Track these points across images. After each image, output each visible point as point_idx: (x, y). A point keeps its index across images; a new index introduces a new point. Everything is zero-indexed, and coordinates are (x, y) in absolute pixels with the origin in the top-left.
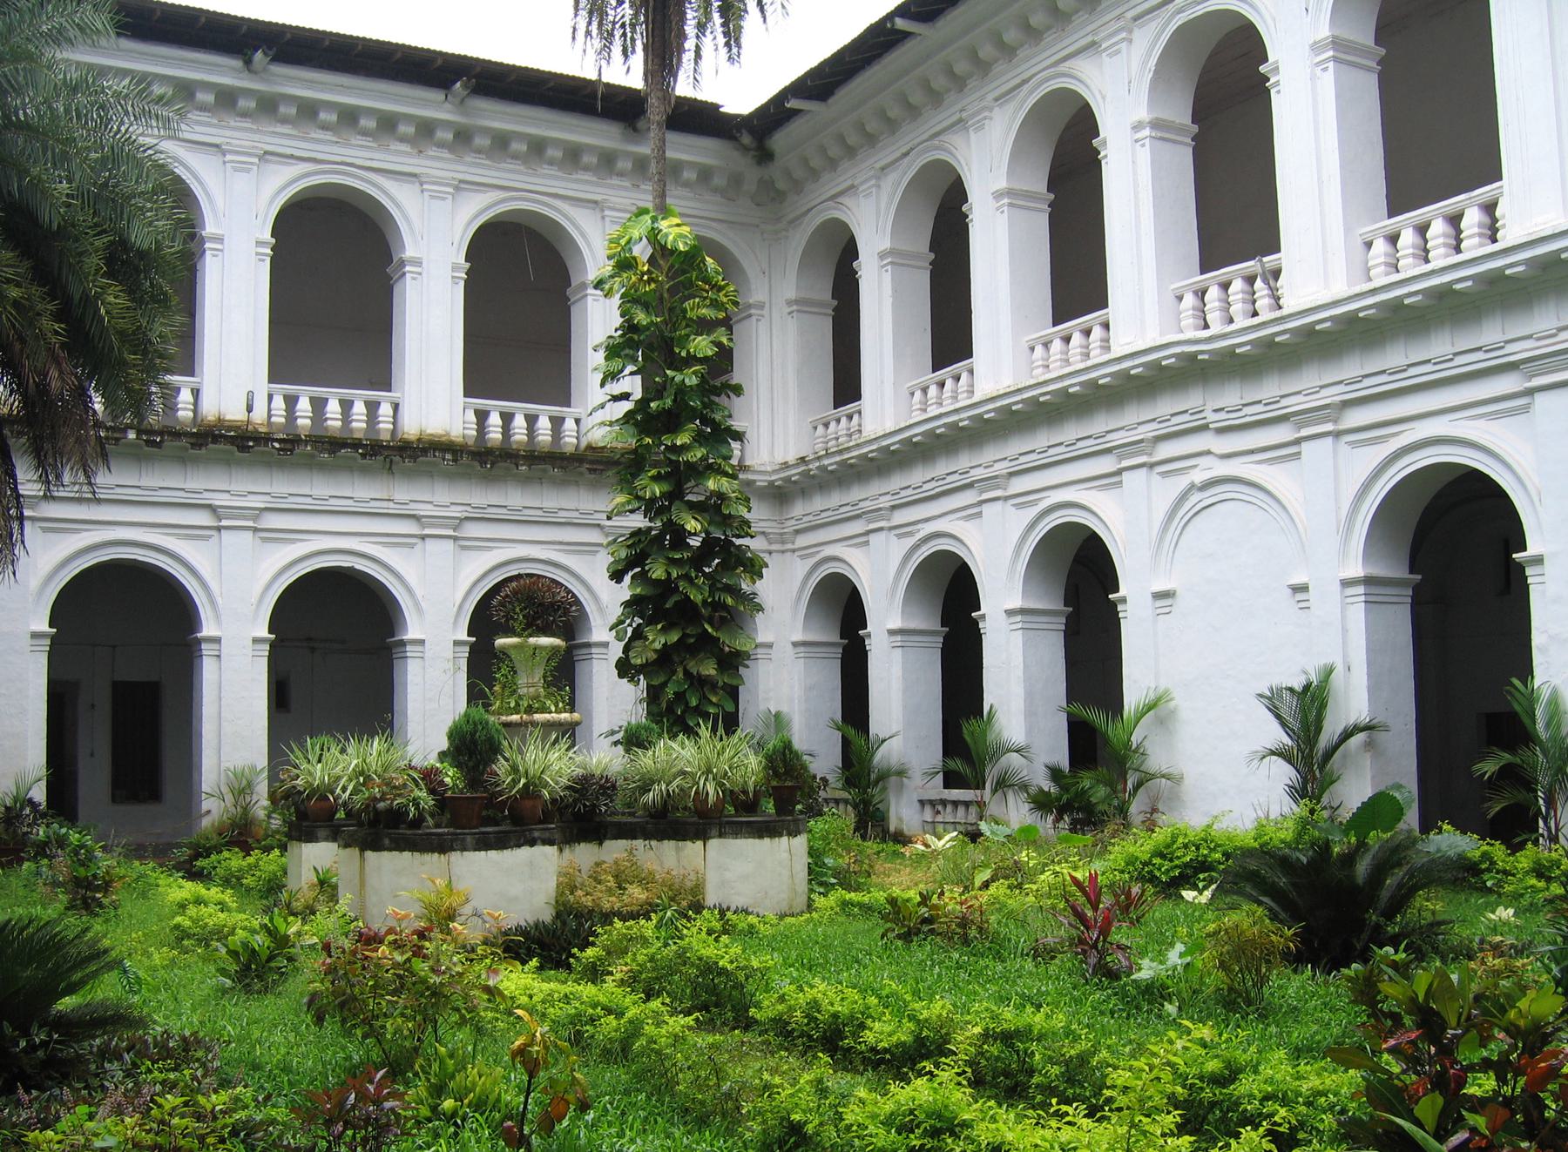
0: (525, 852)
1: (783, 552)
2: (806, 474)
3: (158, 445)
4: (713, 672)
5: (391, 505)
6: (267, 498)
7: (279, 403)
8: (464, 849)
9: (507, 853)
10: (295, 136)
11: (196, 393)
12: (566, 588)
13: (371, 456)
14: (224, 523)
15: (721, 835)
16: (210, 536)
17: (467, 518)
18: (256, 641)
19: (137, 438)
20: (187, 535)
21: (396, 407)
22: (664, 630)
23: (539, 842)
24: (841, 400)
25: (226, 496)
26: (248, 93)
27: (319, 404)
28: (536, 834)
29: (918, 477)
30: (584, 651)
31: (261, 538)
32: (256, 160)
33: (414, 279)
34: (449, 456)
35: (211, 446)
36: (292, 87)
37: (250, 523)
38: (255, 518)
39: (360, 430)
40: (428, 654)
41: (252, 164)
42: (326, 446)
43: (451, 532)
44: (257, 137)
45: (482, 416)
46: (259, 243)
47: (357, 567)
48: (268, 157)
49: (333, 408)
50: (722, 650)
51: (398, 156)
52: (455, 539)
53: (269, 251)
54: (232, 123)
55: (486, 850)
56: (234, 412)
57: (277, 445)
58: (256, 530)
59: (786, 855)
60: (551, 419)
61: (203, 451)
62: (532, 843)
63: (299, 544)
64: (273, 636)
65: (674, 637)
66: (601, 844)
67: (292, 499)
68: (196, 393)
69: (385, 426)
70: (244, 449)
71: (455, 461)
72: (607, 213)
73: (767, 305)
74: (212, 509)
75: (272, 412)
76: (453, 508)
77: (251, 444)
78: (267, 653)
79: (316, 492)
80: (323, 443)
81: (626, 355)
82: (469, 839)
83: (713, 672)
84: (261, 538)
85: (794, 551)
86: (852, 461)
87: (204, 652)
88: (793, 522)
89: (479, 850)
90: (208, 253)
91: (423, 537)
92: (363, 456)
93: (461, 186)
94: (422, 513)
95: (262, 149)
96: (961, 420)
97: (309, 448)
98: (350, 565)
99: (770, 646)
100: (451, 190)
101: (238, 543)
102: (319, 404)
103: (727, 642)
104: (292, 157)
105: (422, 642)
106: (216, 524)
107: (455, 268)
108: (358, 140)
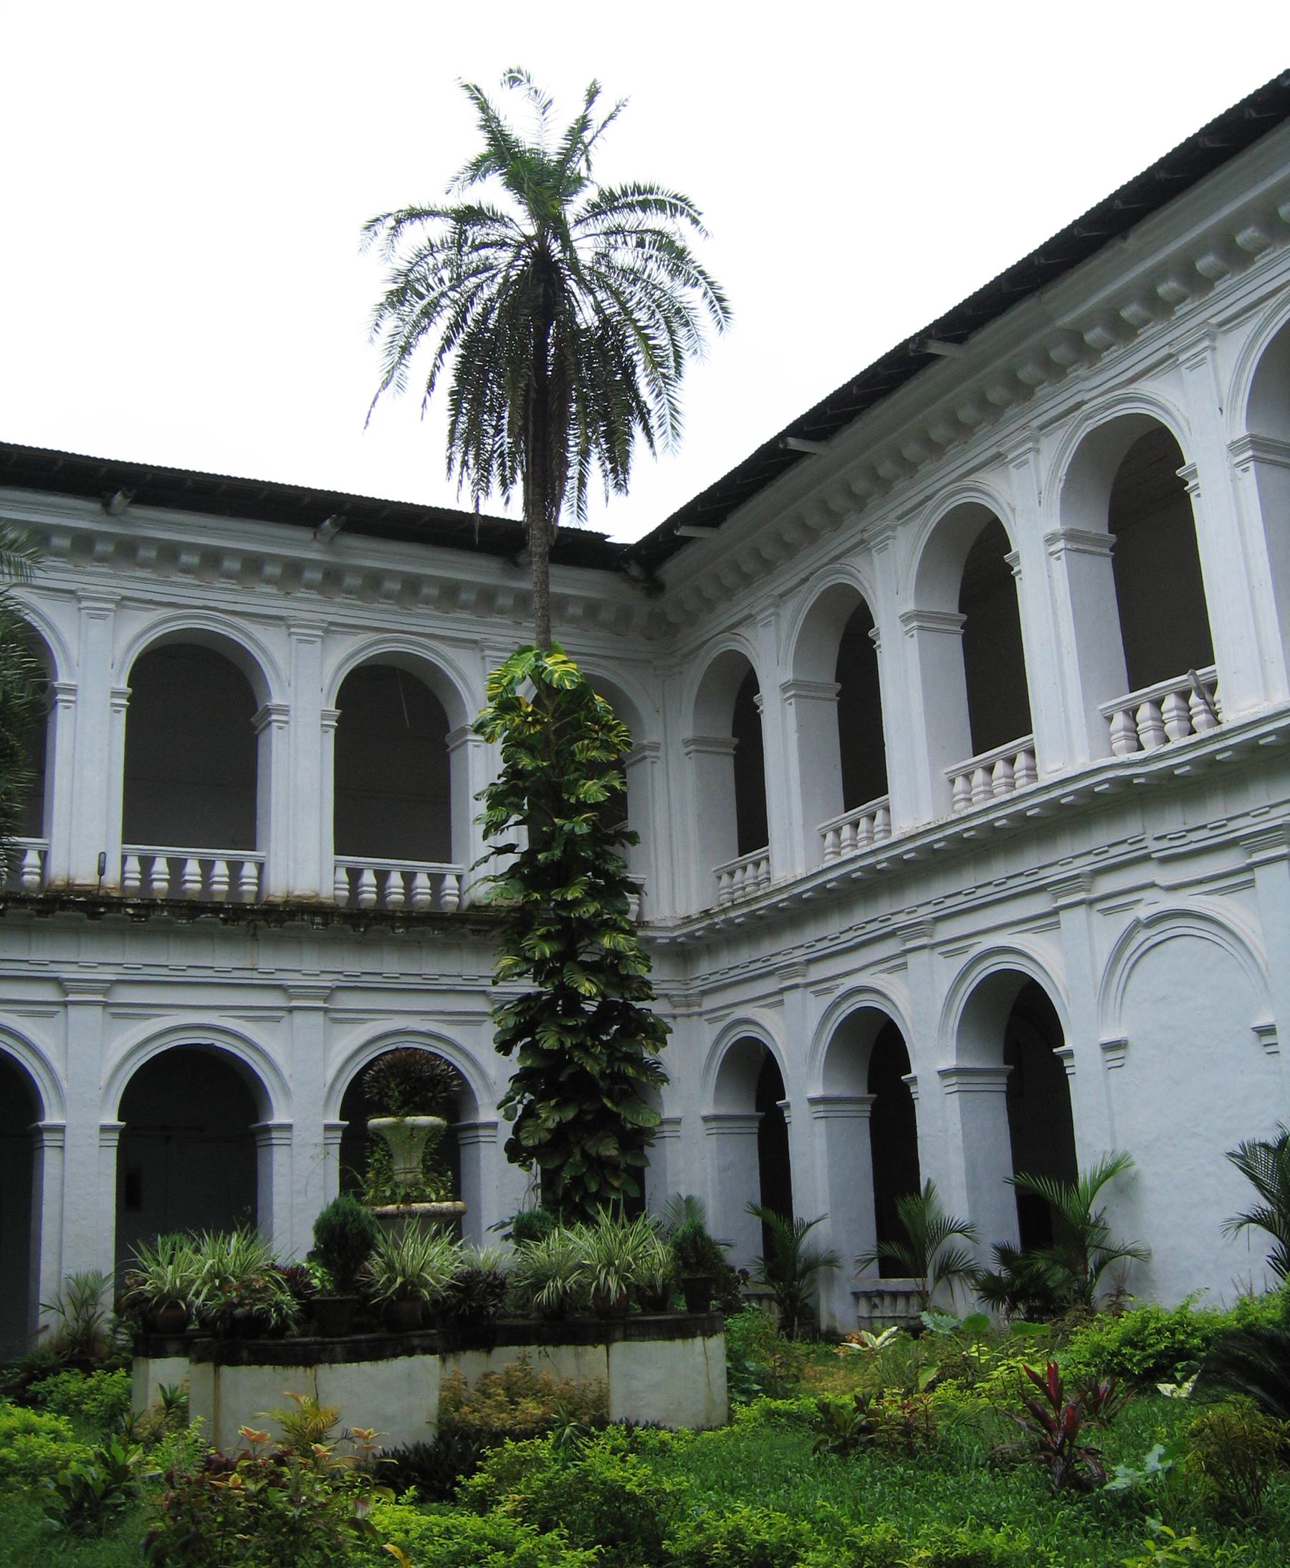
0: (401, 1364)
1: (689, 1016)
2: (710, 928)
4: (614, 1152)
5: (255, 974)
6: (120, 970)
7: (133, 865)
8: (333, 1361)
9: (382, 1365)
10: (154, 580)
11: (44, 855)
12: (446, 1060)
13: (234, 921)
14: (72, 998)
15: (627, 1338)
17: (339, 988)
18: (105, 1129)
21: (261, 867)
22: (558, 1107)
23: (419, 1351)
24: (744, 848)
25: (74, 968)
27: (177, 866)
28: (416, 1342)
29: (834, 927)
30: (470, 1134)
31: (112, 1014)
33: (280, 728)
34: (318, 920)
36: (148, 528)
37: (100, 998)
38: (106, 992)
39: (221, 892)
40: (296, 1141)
42: (184, 911)
43: (320, 1004)
44: (114, 582)
45: (354, 874)
46: (115, 694)
47: (218, 1044)
49: (193, 868)
50: (623, 1127)
51: (264, 599)
52: (326, 1010)
53: (124, 702)
55: (358, 1361)
56: (85, 875)
57: (130, 911)
58: (106, 1005)
59: (701, 1359)
60: (431, 876)
61: (50, 919)
62: (410, 1352)
64: (123, 1123)
65: (570, 1114)
66: (489, 1352)
68: (44, 855)
69: (249, 888)
70: (94, 915)
71: (325, 924)
72: (487, 652)
73: (663, 746)
74: (58, 982)
75: (127, 875)
76: (323, 977)
78: (116, 1143)
79: (172, 961)
80: (181, 907)
81: (511, 804)
82: (339, 1349)
83: (614, 1152)
84: (112, 1014)
85: (700, 1014)
86: (761, 912)
87: (46, 1143)
88: (699, 982)
89: (351, 1361)
90: (60, 704)
91: (291, 1010)
92: (225, 921)
93: (331, 629)
94: (290, 983)
96: (879, 862)
97: (165, 914)
98: (209, 1042)
99: (677, 1122)
100: (320, 633)
101: (86, 1019)
102: (177, 866)
103: (629, 1118)
105: (288, 1127)
106: (62, 999)
107: (324, 716)
108: (222, 583)
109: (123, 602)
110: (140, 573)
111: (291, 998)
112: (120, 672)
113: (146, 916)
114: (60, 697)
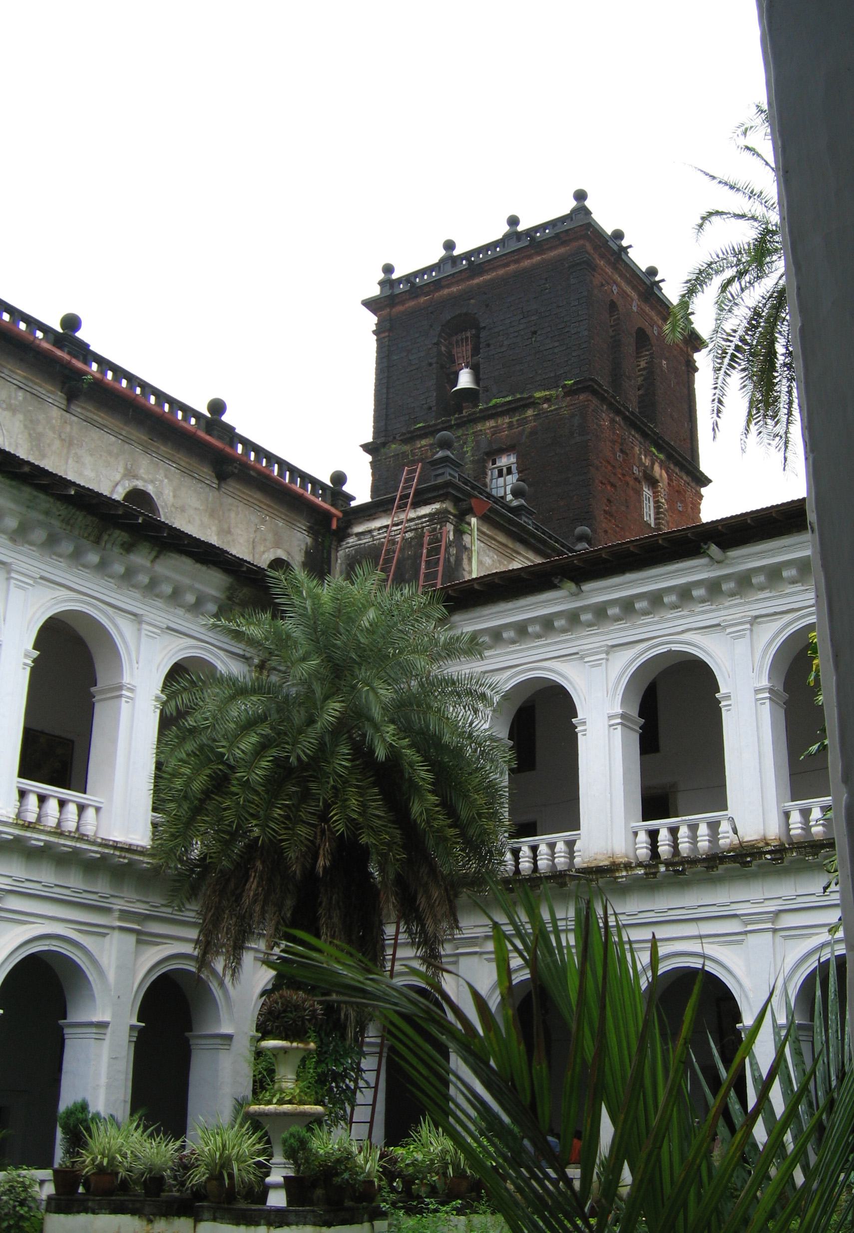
3: (682, 872)
6: (780, 902)
10: (774, 597)
16: (743, 941)
19: (667, 870)
20: (725, 942)
25: (748, 905)
26: (727, 577)
32: (748, 626)
35: (720, 867)
36: (749, 562)
37: (769, 925)
41: (743, 630)
42: (808, 850)
44: (747, 608)
46: (757, 691)
48: (759, 620)
53: (767, 695)
54: (727, 604)
56: (773, 830)
57: (768, 856)
63: (815, 937)
67: (800, 900)
77: (749, 859)
80: (805, 847)
90: (723, 709)
95: (749, 616)
97: (795, 854)
104: (776, 614)
109: (755, 620)
110: (762, 595)
111: (746, 924)
112: (761, 671)
113: (782, 859)
114: (723, 703)
